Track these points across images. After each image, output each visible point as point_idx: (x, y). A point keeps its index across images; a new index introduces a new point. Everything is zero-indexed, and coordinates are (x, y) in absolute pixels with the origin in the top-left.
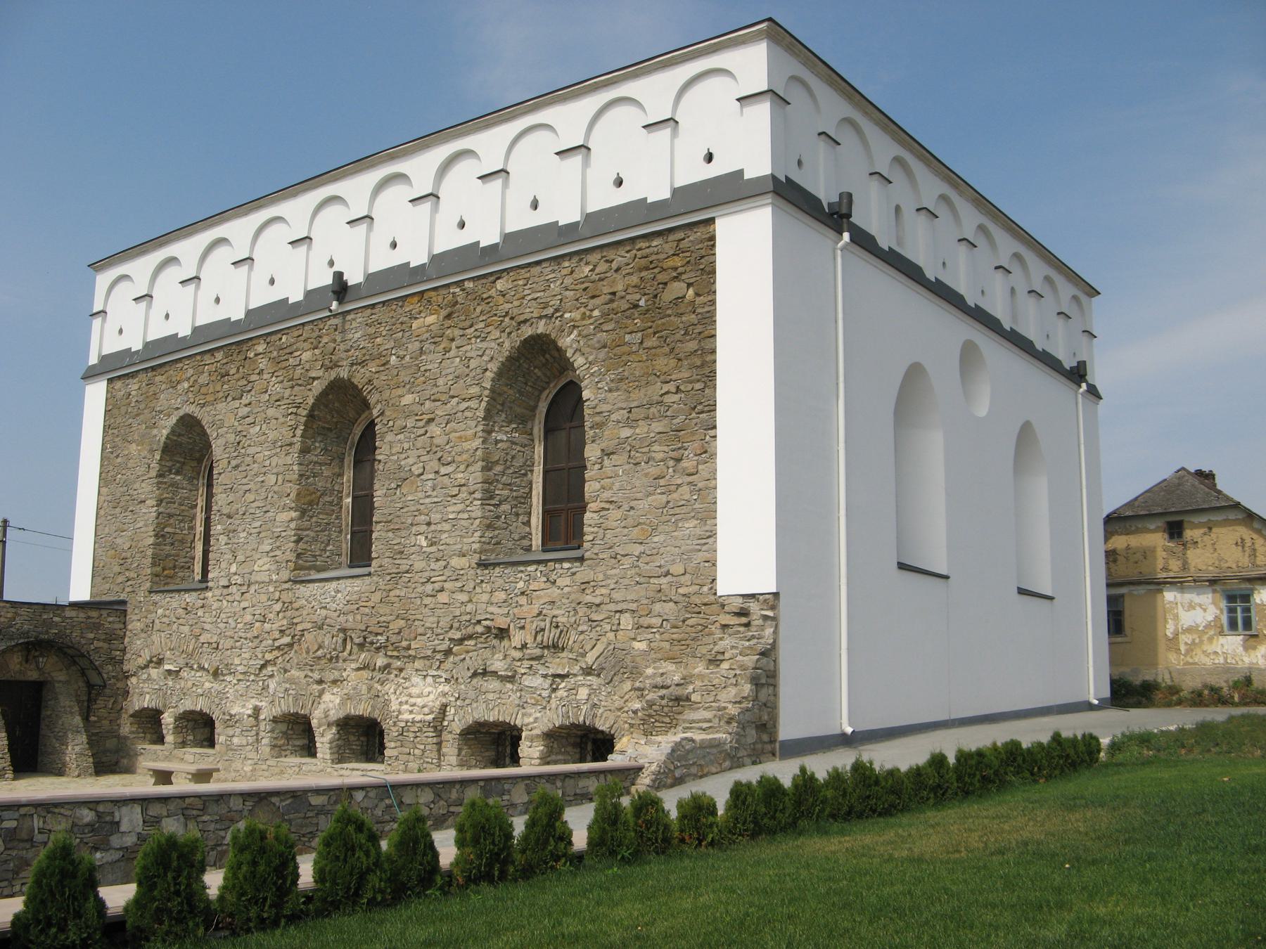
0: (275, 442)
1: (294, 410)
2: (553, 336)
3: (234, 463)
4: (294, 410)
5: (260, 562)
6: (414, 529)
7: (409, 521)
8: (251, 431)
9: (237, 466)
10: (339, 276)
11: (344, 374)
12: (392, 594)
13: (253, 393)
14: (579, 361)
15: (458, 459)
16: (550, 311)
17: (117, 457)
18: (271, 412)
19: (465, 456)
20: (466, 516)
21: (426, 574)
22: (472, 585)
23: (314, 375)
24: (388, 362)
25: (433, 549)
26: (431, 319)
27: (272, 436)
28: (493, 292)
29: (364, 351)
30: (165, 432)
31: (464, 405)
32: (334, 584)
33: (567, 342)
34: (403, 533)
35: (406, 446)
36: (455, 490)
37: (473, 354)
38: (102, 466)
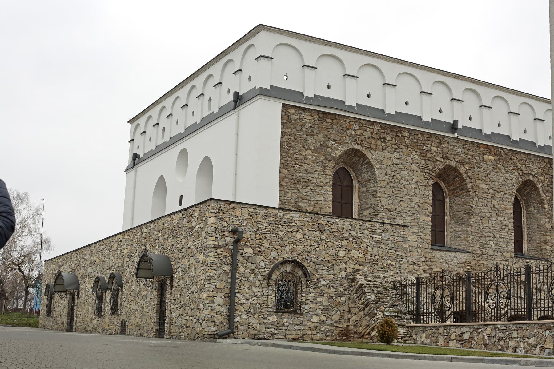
0: (417, 182)
1: (429, 171)
2: (536, 182)
3: (392, 185)
4: (429, 171)
5: (411, 237)
6: (488, 238)
7: (487, 234)
8: (402, 172)
9: (393, 187)
10: (456, 122)
11: (454, 164)
12: (479, 262)
13: (401, 153)
14: (543, 195)
15: (504, 215)
16: (534, 173)
17: (295, 153)
18: (414, 167)
19: (507, 215)
20: (508, 238)
21: (495, 257)
22: (512, 263)
23: (438, 159)
24: (474, 167)
25: (496, 247)
26: (492, 158)
27: (416, 179)
28: (515, 158)
29: (461, 158)
30: (338, 153)
31: (505, 196)
32: (453, 254)
33: (539, 186)
34: (484, 239)
35: (484, 204)
36: (504, 227)
37: (509, 178)
38: (281, 155)
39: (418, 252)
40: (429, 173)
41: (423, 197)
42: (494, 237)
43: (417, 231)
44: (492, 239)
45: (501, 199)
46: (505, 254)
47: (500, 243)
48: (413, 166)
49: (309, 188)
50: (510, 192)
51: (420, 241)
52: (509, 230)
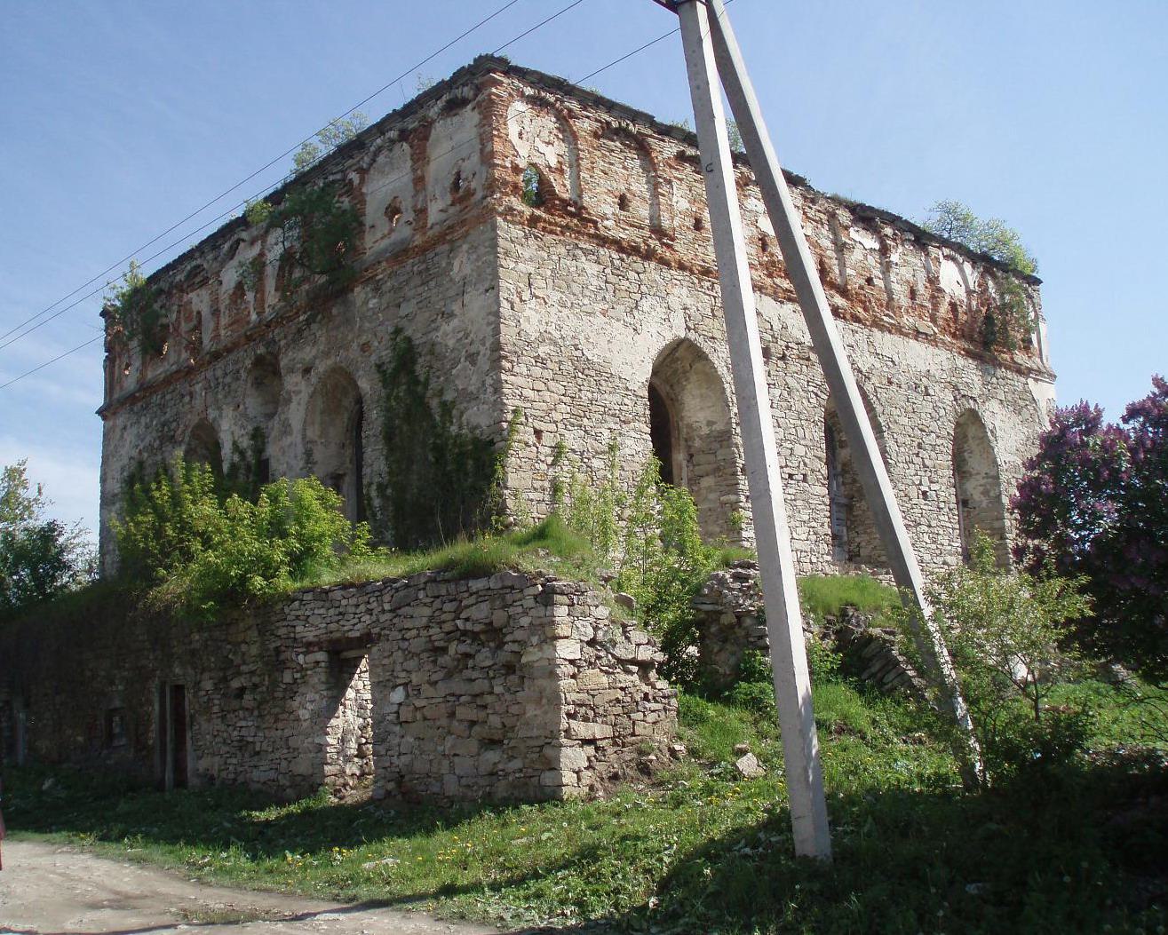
0: (799, 413)
25: (934, 546)
36: (942, 505)
37: (940, 405)
39: (811, 563)
40: (816, 395)
41: (810, 444)
42: (929, 526)
43: (806, 518)
44: (926, 529)
45: (934, 447)
46: (949, 559)
47: (940, 537)
48: (789, 380)
49: (606, 425)
50: (944, 433)
51: (813, 538)
52: (950, 510)
